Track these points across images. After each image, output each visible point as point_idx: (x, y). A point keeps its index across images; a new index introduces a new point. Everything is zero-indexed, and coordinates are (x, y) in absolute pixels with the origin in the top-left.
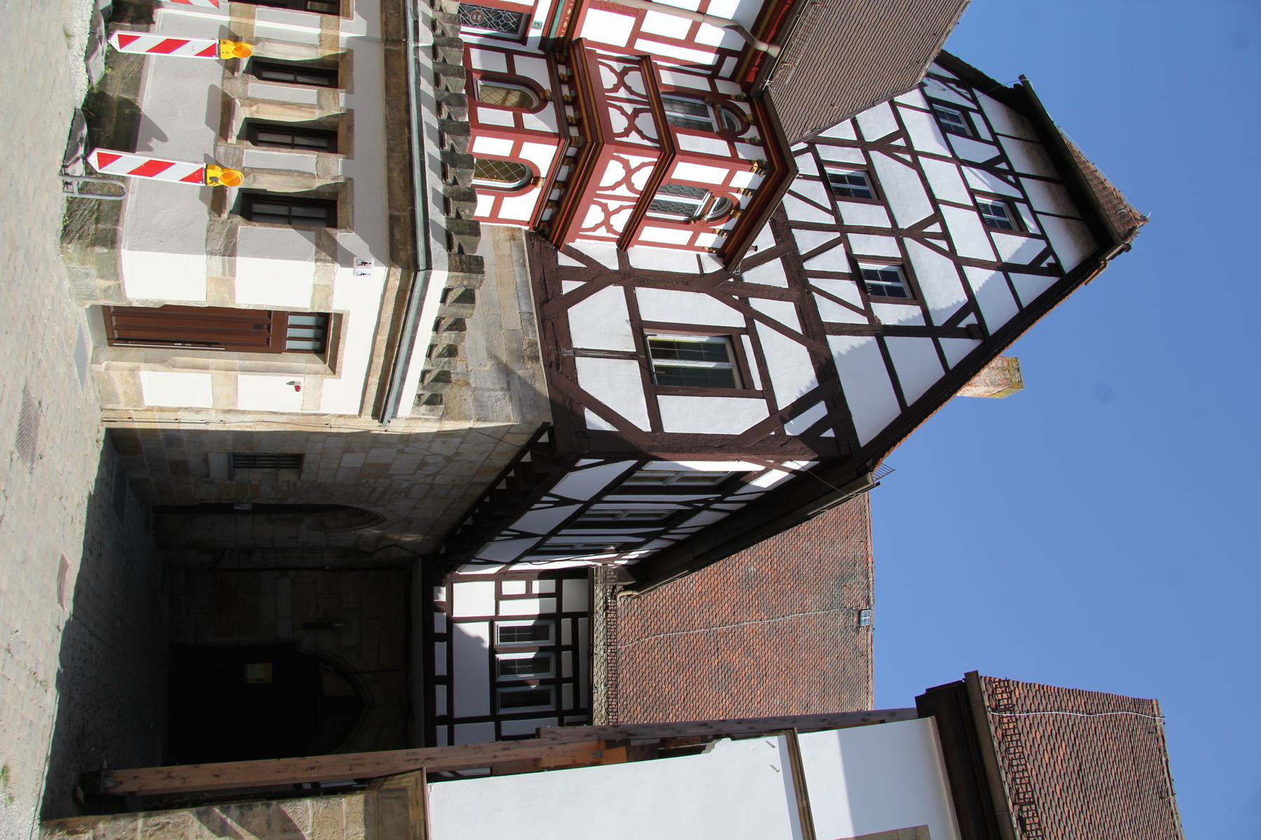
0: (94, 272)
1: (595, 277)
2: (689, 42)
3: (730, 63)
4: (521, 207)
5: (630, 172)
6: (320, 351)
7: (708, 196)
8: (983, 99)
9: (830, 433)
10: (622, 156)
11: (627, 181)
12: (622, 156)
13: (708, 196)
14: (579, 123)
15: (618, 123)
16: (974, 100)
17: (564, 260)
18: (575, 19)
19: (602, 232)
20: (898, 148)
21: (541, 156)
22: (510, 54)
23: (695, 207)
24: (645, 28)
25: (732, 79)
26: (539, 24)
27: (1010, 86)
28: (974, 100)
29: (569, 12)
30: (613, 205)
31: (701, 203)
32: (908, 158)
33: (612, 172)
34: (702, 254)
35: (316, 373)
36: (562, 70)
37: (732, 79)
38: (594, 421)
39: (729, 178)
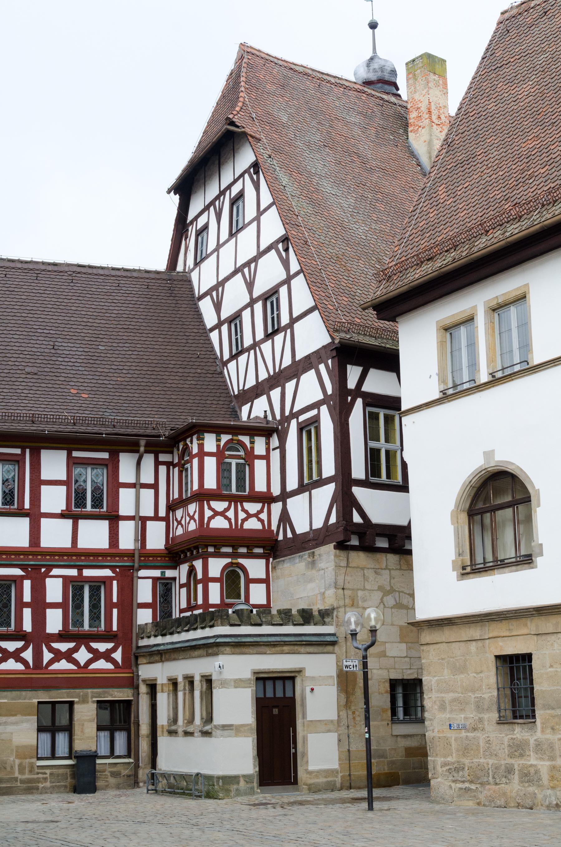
0: (235, 787)
1: (285, 517)
2: (155, 486)
3: (163, 457)
4: (255, 567)
5: (216, 513)
6: (293, 679)
7: (227, 460)
8: (190, 217)
9: (330, 361)
10: (206, 522)
11: (223, 514)
12: (206, 522)
13: (227, 460)
14: (197, 548)
15: (192, 526)
16: (192, 222)
17: (281, 537)
18: (155, 554)
19: (264, 516)
20: (218, 296)
21: (216, 566)
23: (237, 464)
24: (152, 514)
25: (172, 453)
26: (163, 573)
27: (178, 196)
28: (192, 222)
29: (151, 559)
30: (242, 515)
31: (234, 462)
32: (220, 289)
33: (219, 523)
34: (271, 448)
35: (302, 680)
37: (172, 453)
38: (333, 519)
39: (210, 454)
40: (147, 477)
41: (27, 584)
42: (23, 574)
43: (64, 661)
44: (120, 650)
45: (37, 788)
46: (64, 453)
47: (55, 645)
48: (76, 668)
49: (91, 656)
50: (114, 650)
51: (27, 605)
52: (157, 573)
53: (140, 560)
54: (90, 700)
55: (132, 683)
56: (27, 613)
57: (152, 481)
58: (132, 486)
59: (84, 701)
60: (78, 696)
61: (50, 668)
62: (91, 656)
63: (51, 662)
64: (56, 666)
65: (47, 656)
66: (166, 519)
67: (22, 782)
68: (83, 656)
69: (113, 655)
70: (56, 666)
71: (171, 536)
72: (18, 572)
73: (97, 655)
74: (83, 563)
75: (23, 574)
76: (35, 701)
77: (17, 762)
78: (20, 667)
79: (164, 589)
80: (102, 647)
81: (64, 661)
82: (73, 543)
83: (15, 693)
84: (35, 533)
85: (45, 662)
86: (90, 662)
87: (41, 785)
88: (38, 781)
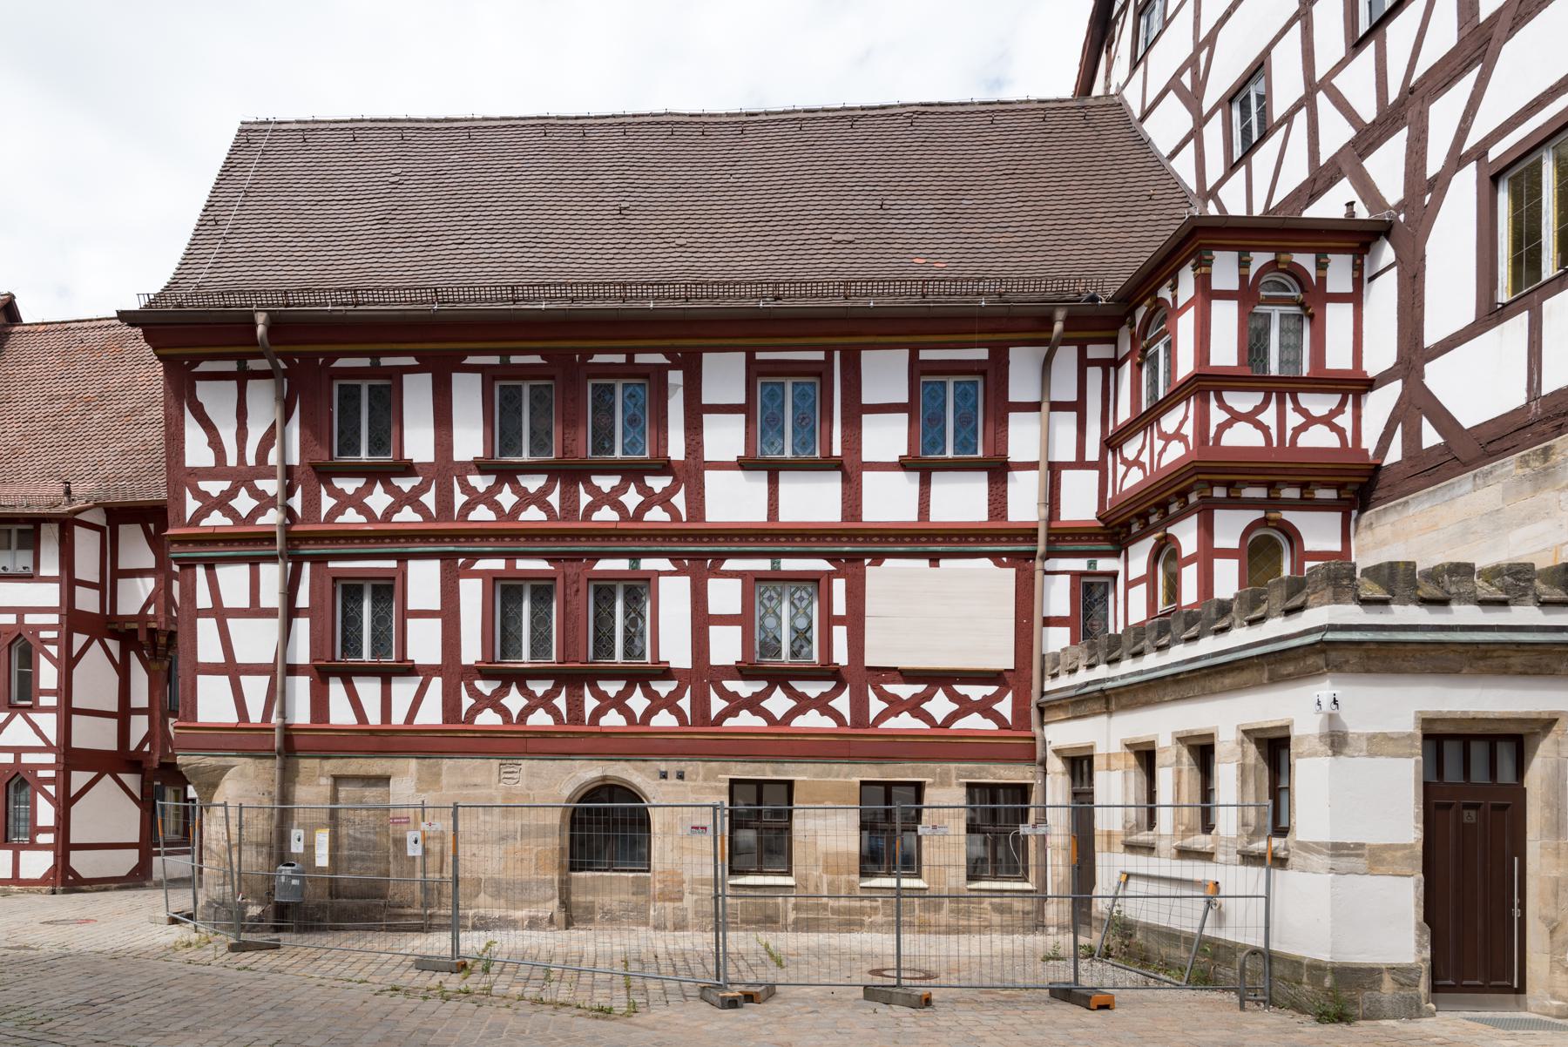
2: (1079, 407)
3: (1094, 351)
22: (1129, 585)
24: (1072, 458)
25: (1114, 341)
26: (1090, 564)
36: (1135, 528)
37: (1114, 341)
40: (1065, 389)
41: (839, 586)
42: (832, 568)
43: (905, 716)
44: (1009, 697)
45: (862, 924)
46: (904, 354)
47: (890, 688)
49: (955, 707)
50: (998, 697)
51: (840, 621)
52: (1080, 564)
53: (1049, 542)
54: (954, 781)
55: (1030, 753)
56: (840, 634)
57: (1073, 397)
58: (1035, 407)
59: (944, 782)
60: (932, 774)
62: (955, 707)
63: (883, 716)
64: (892, 723)
65: (876, 706)
66: (1101, 466)
67: (836, 911)
68: (940, 706)
69: (996, 707)
70: (892, 723)
71: (1110, 495)
72: (822, 565)
73: (966, 707)
75: (832, 568)
76: (857, 780)
77: (825, 878)
78: (828, 723)
79: (1091, 595)
80: (976, 692)
81: (905, 716)
82: (920, 513)
83: (819, 767)
86: (953, 717)
87: (867, 920)
88: (862, 911)
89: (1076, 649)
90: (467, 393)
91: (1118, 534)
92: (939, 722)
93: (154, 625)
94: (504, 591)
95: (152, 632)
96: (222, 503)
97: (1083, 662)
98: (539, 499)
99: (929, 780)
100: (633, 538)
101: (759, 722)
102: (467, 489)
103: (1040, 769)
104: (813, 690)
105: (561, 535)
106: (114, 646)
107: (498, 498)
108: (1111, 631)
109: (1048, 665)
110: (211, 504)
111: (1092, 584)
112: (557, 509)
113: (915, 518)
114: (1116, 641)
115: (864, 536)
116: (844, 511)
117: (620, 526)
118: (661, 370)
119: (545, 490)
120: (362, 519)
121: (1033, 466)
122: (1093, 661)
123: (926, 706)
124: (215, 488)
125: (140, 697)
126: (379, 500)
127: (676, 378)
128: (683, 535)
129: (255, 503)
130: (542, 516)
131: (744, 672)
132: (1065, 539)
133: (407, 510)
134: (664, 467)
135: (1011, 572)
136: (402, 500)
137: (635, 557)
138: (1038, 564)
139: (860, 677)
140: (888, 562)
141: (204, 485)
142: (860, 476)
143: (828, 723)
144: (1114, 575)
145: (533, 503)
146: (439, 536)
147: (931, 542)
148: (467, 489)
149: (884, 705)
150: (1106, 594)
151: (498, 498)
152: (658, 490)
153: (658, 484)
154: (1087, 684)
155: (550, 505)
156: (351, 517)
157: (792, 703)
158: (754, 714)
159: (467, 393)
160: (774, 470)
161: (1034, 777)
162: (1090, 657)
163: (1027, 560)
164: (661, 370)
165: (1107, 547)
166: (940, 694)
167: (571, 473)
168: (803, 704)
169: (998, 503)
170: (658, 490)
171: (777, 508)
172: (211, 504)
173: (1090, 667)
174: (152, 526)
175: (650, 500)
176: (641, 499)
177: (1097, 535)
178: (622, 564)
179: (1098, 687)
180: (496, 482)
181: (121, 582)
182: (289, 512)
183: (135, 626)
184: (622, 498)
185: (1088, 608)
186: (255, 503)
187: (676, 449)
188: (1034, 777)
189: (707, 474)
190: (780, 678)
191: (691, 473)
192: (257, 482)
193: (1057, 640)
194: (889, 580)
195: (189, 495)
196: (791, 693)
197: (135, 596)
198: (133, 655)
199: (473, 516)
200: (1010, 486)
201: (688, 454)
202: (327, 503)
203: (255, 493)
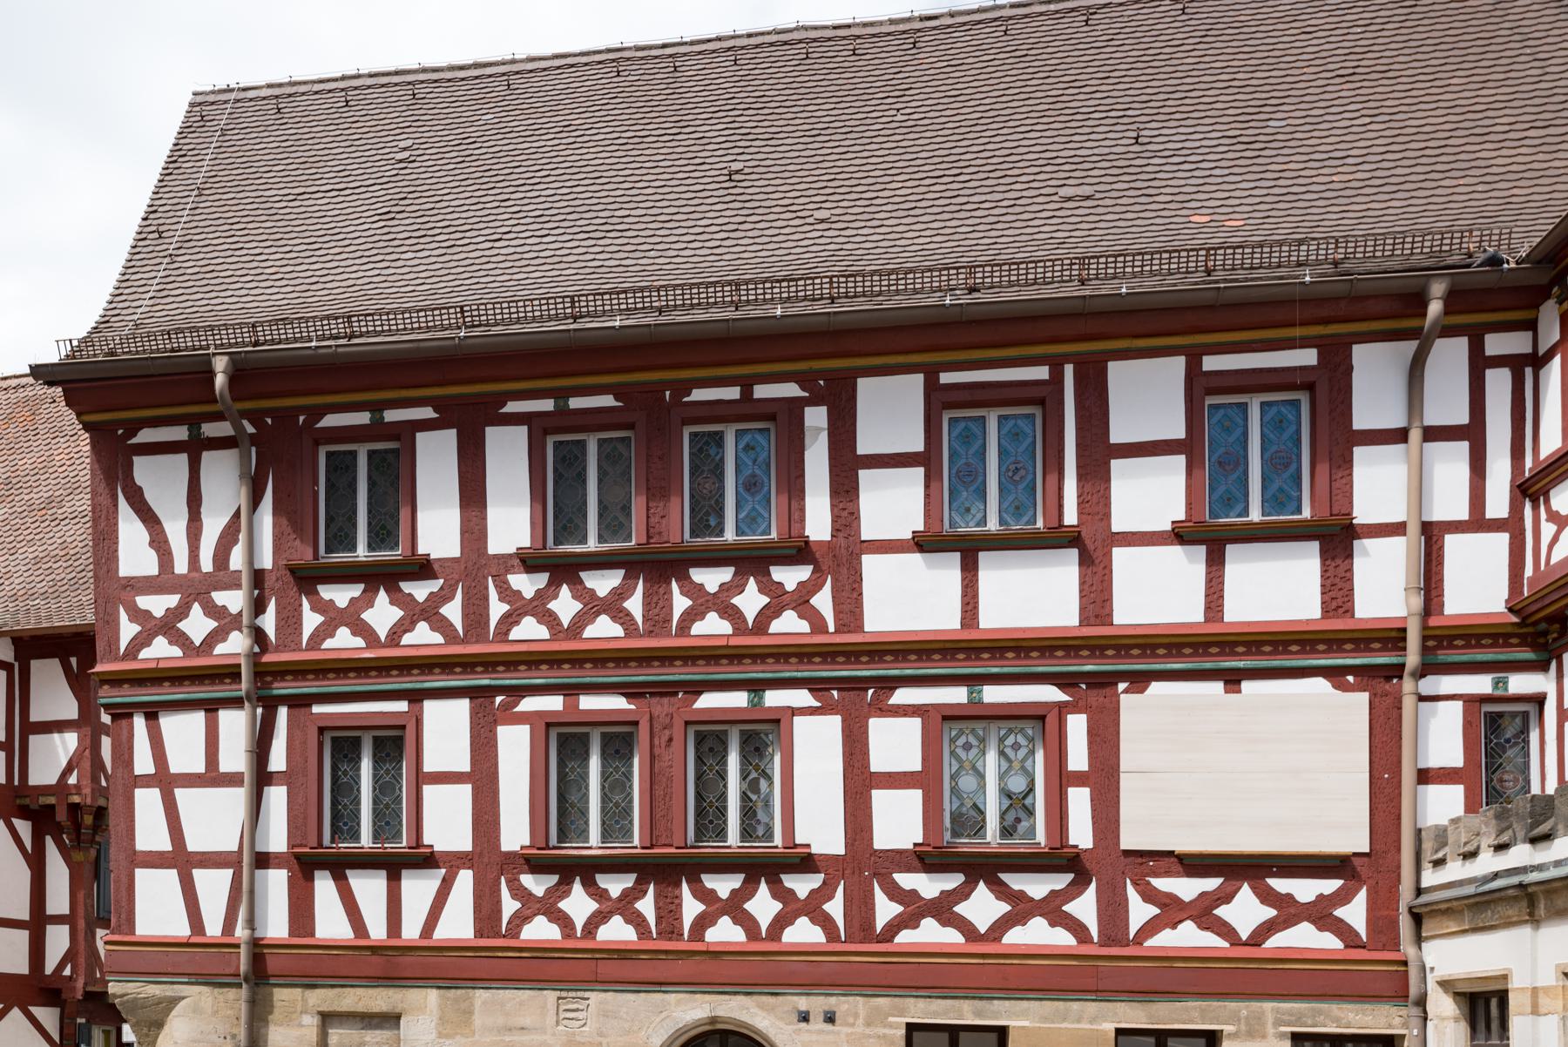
41: (1077, 726)
47: (1162, 884)
48: (1227, 945)
51: (1080, 779)
56: (1079, 801)
61: (1149, 943)
63: (1151, 928)
64: (1166, 939)
65: (1140, 912)
70: (1166, 939)
74: (1241, 664)
76: (1109, 1027)
78: (1062, 938)
82: (1208, 608)
84: (1096, 592)
85: (1134, 925)
89: (1475, 820)
90: (507, 453)
91: (1545, 633)
92: (1244, 938)
93: (76, 799)
94: (564, 742)
95: (74, 809)
96: (168, 626)
97: (1487, 841)
98: (613, 606)
99: (1228, 1029)
100: (753, 660)
101: (953, 937)
102: (507, 593)
103: (1415, 1011)
104: (1037, 887)
105: (645, 658)
106: (24, 828)
107: (553, 605)
108: (1535, 789)
109: (1428, 846)
110: (152, 628)
111: (1500, 715)
112: (639, 619)
113: (1199, 617)
114: (1544, 807)
115: (1117, 648)
116: (1082, 609)
117: (734, 642)
118: (794, 409)
119: (621, 594)
120: (359, 642)
121: (1397, 529)
122: (1505, 838)
123: (1222, 912)
124: (158, 605)
125: (58, 899)
126: (383, 614)
127: (816, 418)
128: (830, 654)
129: (212, 624)
130: (618, 631)
131: (927, 859)
132: (1452, 644)
133: (422, 626)
134: (800, 552)
135: (1360, 701)
136: (415, 613)
137: (756, 687)
138: (1408, 685)
139: (1115, 866)
140: (1156, 687)
141: (144, 602)
142: (1109, 555)
143: (1062, 938)
144: (1539, 700)
145: (603, 612)
146: (468, 664)
147: (1226, 654)
148: (507, 593)
149: (1154, 911)
150: (1525, 730)
151: (553, 605)
152: (790, 586)
153: (790, 577)
154: (1496, 875)
155: (628, 614)
156: (344, 641)
157: (1004, 908)
158: (944, 923)
159: (507, 453)
160: (969, 550)
161: (1405, 1025)
162: (1500, 832)
163: (1388, 679)
164: (794, 409)
165: (1528, 655)
166: (1245, 893)
167: (658, 566)
168: (1022, 908)
169: (1337, 590)
170: (790, 586)
171: (976, 607)
172: (152, 628)
173: (1501, 848)
174: (74, 660)
175: (779, 601)
176: (766, 600)
177: (1507, 636)
178: (738, 700)
179: (1515, 880)
180: (550, 584)
181: (34, 740)
182: (259, 635)
183: (52, 800)
184: (736, 601)
185: (1494, 755)
186: (212, 624)
187: (818, 524)
188: (1405, 1025)
189: (867, 560)
190: (984, 869)
191: (842, 560)
192: (214, 595)
193: (1443, 805)
194: (1155, 715)
195: (123, 616)
196: (1002, 891)
197: (52, 758)
198: (49, 842)
199: (515, 634)
200: (1358, 563)
201: (836, 531)
202: (311, 621)
203: (212, 611)
